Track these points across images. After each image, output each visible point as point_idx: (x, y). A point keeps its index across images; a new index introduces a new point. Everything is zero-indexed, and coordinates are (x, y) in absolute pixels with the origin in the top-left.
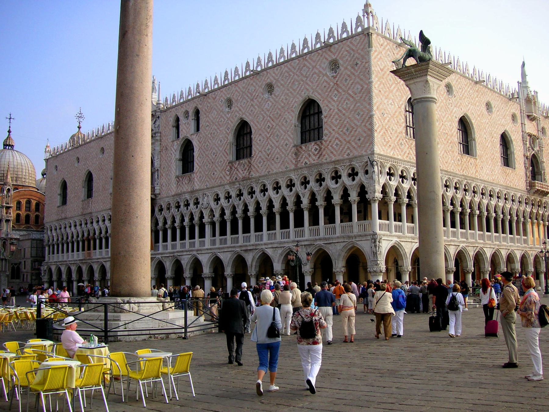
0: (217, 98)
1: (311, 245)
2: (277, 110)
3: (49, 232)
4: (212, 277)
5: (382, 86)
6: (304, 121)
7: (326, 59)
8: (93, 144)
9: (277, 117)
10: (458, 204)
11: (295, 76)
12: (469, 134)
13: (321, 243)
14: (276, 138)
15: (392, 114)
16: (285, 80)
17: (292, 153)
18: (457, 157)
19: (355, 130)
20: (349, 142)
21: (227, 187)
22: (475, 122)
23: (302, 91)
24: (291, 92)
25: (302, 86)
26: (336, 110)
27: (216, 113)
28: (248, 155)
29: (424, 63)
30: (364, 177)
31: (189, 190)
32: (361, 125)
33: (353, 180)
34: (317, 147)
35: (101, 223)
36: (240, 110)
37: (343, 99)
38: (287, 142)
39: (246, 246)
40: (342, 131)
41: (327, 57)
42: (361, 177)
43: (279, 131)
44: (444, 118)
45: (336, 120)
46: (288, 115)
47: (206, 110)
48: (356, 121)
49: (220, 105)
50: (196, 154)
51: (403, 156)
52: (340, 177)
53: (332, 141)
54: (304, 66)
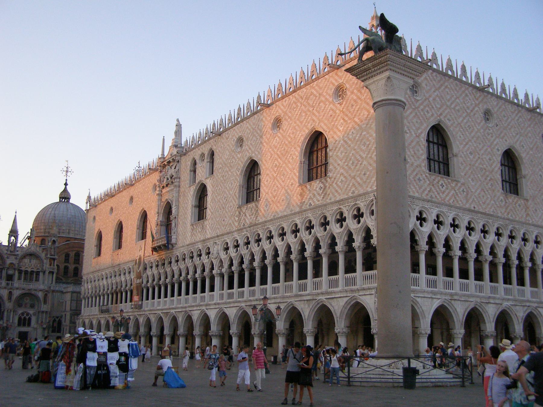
0: (230, 137)
1: (313, 300)
3: (86, 284)
4: (220, 336)
6: (311, 157)
7: (333, 84)
8: (124, 193)
10: (500, 254)
11: (303, 107)
12: (517, 171)
13: (323, 298)
14: (282, 177)
16: (293, 112)
17: (297, 194)
18: (499, 197)
19: (360, 163)
20: (354, 178)
22: (524, 155)
23: (309, 123)
24: (298, 125)
25: (308, 117)
26: (342, 142)
27: (228, 154)
29: (381, 54)
30: (369, 219)
31: (202, 239)
32: (366, 157)
33: (359, 222)
34: (322, 186)
35: (127, 274)
36: (250, 149)
37: (349, 129)
38: (292, 181)
39: (251, 301)
40: (347, 165)
41: (334, 81)
43: (286, 170)
44: (480, 150)
45: (341, 153)
46: (294, 150)
47: (219, 151)
48: (361, 153)
50: (209, 198)
51: (422, 194)
52: (344, 219)
53: (337, 177)
54: (311, 95)
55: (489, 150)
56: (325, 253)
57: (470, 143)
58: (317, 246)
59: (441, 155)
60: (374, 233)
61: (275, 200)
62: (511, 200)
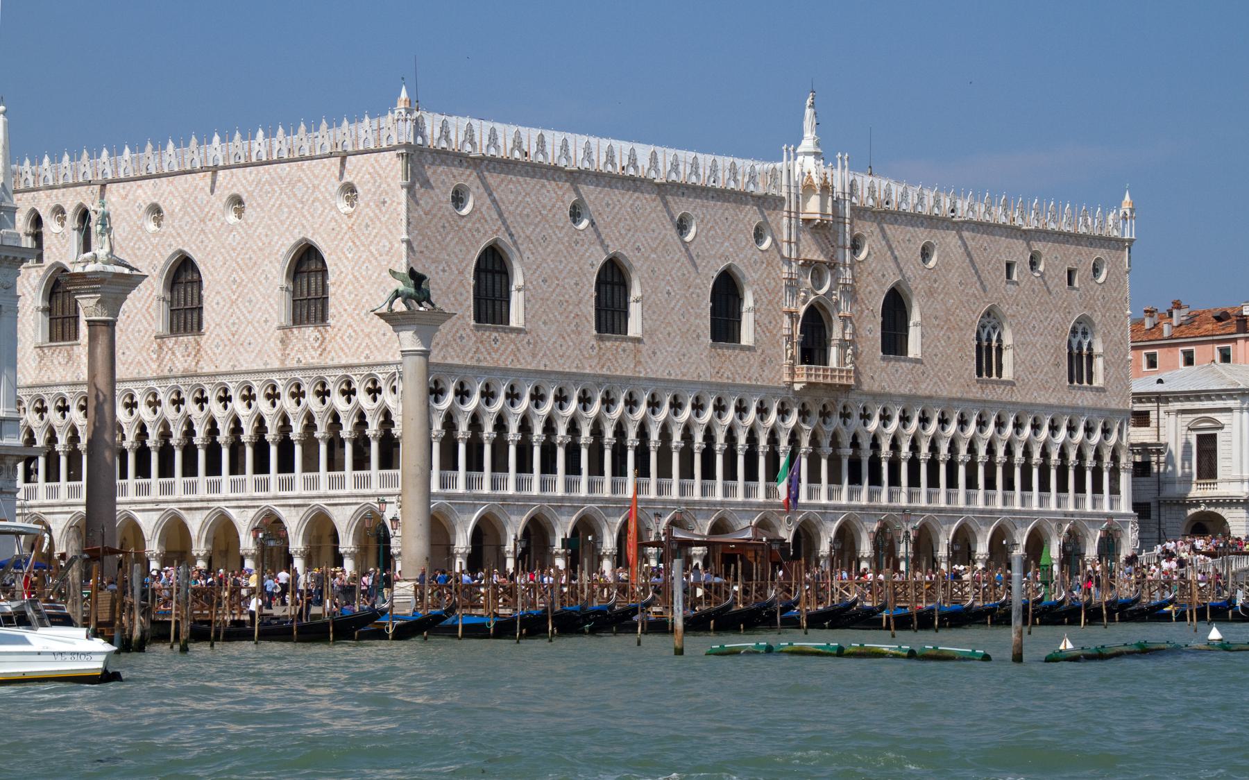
2: (250, 252)
5: (427, 242)
9: (250, 265)
11: (284, 196)
13: (321, 502)
15: (444, 289)
20: (368, 335)
21: (153, 384)
26: (350, 276)
27: (127, 229)
28: (195, 326)
42: (387, 398)
44: (561, 272)
45: (350, 293)
49: (136, 214)
52: (354, 392)
55: (576, 268)
56: (323, 438)
57: (544, 265)
58: (310, 426)
59: (497, 287)
60: (397, 418)
61: (234, 340)
62: (608, 344)
